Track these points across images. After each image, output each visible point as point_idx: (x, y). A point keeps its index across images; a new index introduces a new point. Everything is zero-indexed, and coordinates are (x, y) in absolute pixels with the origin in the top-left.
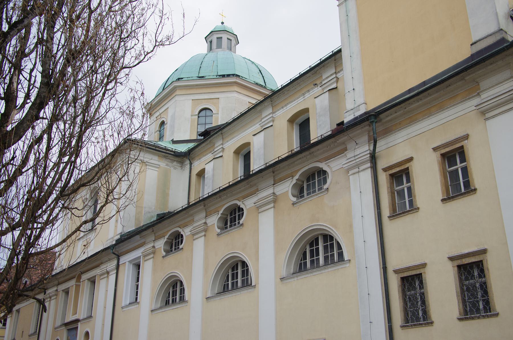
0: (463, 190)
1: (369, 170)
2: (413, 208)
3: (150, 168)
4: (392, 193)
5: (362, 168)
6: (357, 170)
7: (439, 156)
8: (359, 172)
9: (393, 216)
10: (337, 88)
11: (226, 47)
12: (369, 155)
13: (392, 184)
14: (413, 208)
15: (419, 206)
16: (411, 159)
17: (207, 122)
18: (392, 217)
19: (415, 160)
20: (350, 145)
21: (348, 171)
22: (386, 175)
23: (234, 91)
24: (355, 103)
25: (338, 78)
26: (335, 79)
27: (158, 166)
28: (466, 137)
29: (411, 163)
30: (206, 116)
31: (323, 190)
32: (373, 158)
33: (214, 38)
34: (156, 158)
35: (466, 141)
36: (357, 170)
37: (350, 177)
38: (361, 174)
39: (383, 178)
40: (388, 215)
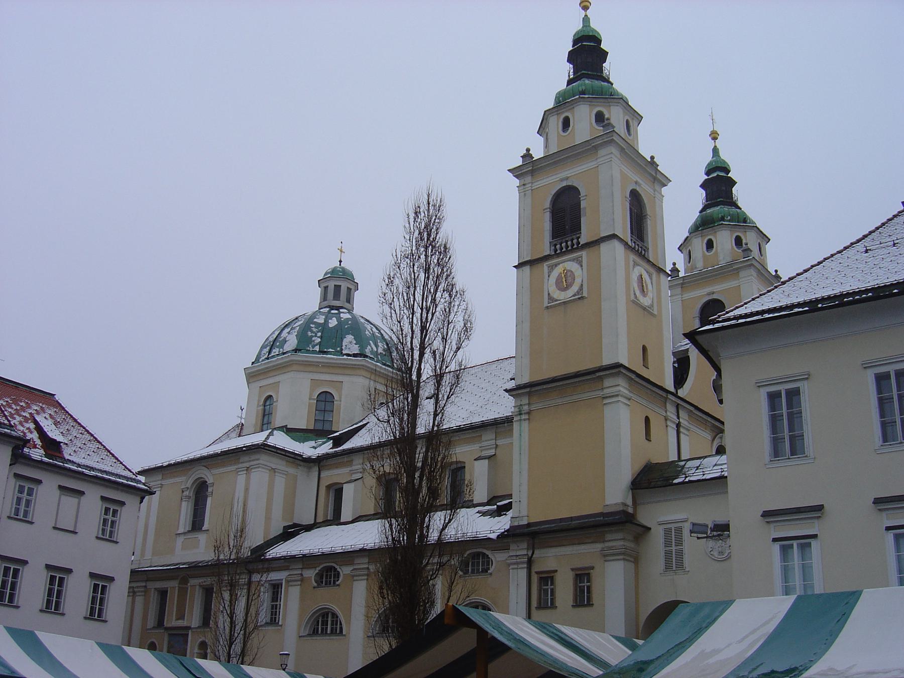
0: (586, 603)
1: (526, 570)
2: (553, 606)
3: (279, 475)
4: (540, 591)
5: (521, 566)
6: (516, 566)
7: (574, 574)
8: (517, 568)
9: (539, 608)
10: (495, 455)
11: (345, 301)
12: (526, 559)
13: (540, 583)
14: (553, 606)
15: (557, 605)
16: (556, 571)
17: (328, 408)
18: (539, 608)
19: (558, 572)
20: (513, 546)
21: (509, 565)
22: (537, 577)
23: (360, 376)
24: (520, 513)
25: (497, 445)
26: (495, 446)
27: (286, 473)
28: (593, 568)
29: (556, 573)
30: (325, 401)
31: (487, 573)
32: (530, 562)
33: (331, 285)
34: (284, 463)
35: (592, 571)
37: (511, 570)
38: (519, 570)
39: (535, 578)
40: (536, 606)
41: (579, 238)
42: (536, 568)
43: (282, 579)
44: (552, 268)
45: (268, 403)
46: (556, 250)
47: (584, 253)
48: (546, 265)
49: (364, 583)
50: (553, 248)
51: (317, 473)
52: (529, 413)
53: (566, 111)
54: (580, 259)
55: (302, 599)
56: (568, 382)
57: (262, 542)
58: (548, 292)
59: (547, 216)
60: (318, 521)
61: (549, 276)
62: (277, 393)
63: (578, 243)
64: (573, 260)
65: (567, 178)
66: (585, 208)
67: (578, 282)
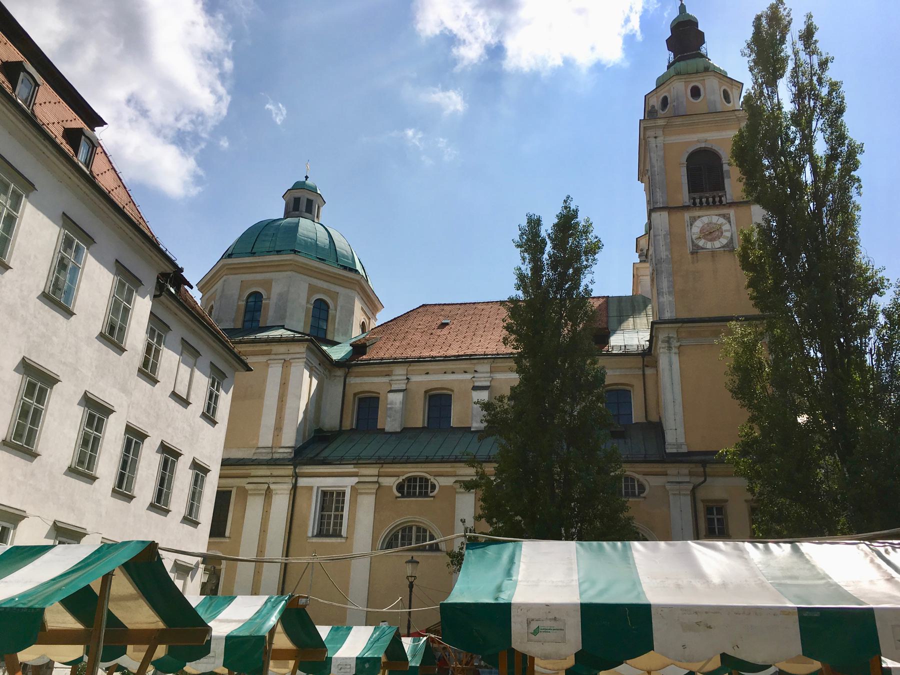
1: (689, 497)
16: (726, 501)
36: (677, 492)
39: (701, 507)
40: (704, 534)
41: (720, 197)
42: (702, 494)
43: (346, 486)
44: (693, 220)
45: (251, 299)
46: (694, 204)
47: (732, 212)
48: (687, 216)
49: (372, 499)
50: (692, 201)
51: (343, 378)
52: (679, 348)
53: (696, 81)
54: (728, 216)
55: (378, 508)
56: (673, 326)
57: (301, 444)
58: (692, 239)
59: (684, 170)
60: (343, 429)
61: (691, 225)
62: (269, 290)
63: (721, 201)
64: (719, 215)
65: (706, 141)
66: (728, 171)
67: (728, 234)
